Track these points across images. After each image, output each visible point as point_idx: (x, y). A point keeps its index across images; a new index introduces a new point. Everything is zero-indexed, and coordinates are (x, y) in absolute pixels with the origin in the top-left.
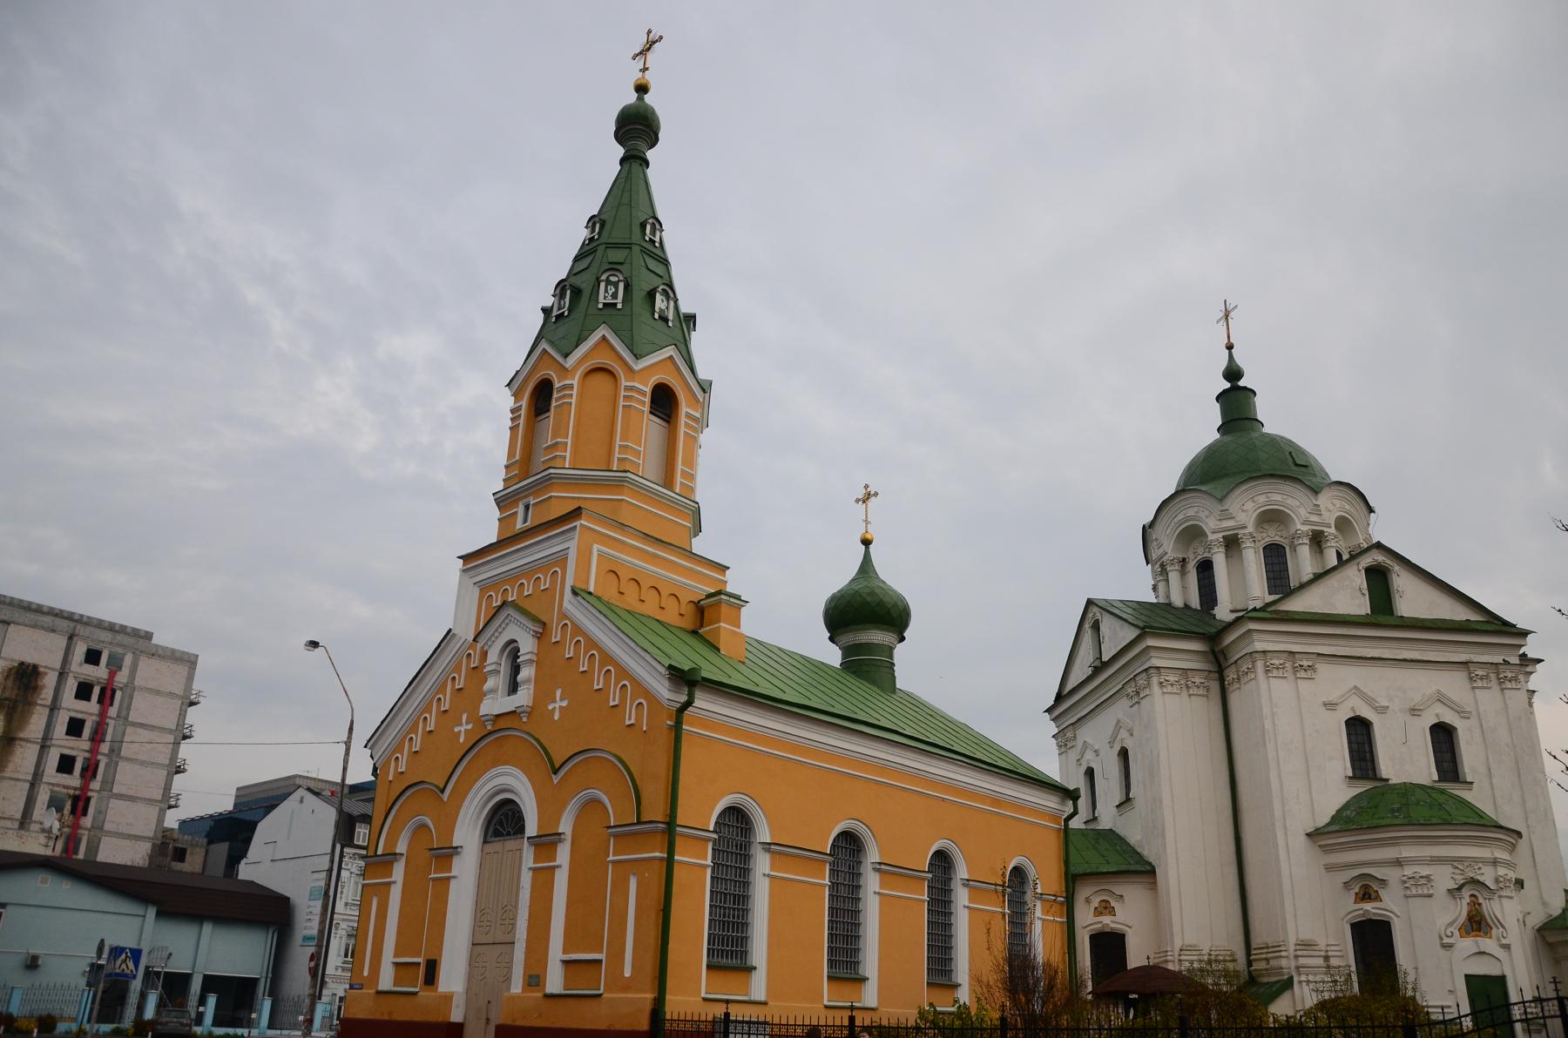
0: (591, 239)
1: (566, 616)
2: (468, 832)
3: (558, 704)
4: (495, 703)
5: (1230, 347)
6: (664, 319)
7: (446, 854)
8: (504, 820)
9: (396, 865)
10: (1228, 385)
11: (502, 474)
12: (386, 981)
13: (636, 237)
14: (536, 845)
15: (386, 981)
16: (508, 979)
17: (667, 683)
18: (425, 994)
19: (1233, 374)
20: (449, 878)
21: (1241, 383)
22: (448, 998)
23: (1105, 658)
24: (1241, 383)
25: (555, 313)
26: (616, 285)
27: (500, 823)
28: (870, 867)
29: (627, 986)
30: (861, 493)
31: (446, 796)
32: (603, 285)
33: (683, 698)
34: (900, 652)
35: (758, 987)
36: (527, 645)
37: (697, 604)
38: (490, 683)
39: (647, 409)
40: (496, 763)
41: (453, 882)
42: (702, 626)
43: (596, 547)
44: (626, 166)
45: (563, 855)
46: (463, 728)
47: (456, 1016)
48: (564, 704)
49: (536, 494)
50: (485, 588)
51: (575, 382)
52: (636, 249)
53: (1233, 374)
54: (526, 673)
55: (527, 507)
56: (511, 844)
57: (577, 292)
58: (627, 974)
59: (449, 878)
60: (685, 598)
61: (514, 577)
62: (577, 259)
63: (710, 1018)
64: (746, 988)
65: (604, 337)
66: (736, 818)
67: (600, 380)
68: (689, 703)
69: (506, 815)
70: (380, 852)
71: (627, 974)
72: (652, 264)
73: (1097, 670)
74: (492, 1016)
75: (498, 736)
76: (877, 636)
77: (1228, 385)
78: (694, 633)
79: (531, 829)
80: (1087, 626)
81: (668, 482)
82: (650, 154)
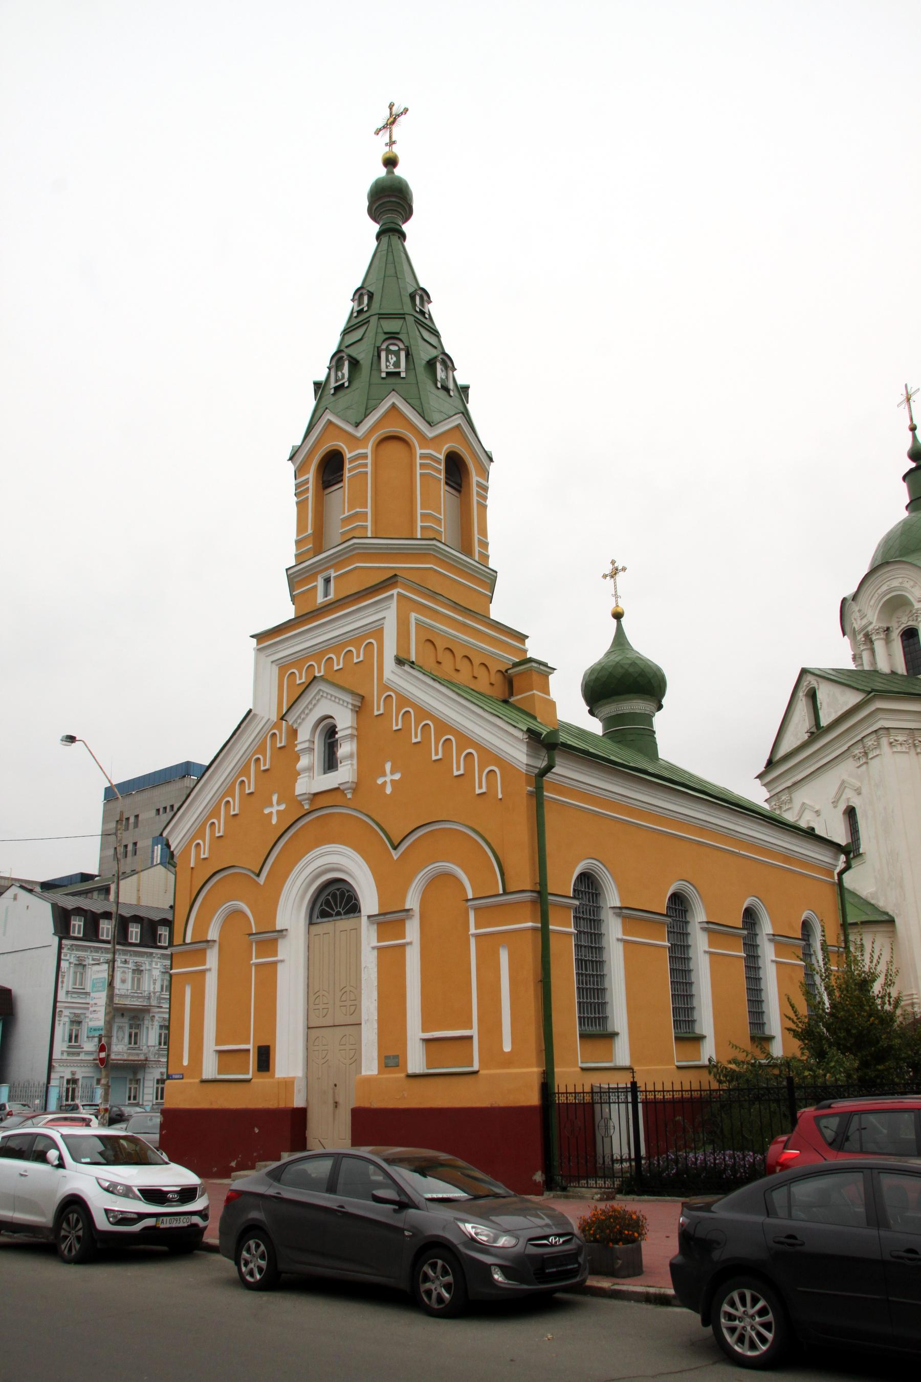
0: (360, 312)
1: (388, 688)
2: (291, 912)
3: (389, 778)
4: (311, 781)
6: (446, 389)
7: (270, 939)
8: (334, 900)
9: (209, 952)
11: (292, 550)
12: (210, 1068)
13: (408, 308)
14: (378, 924)
15: (210, 1069)
16: (356, 1060)
17: (524, 748)
18: (261, 1081)
22: (288, 1084)
23: (824, 722)
25: (333, 384)
26: (397, 354)
27: (327, 903)
28: (698, 927)
30: (608, 569)
31: (262, 880)
32: (383, 355)
33: (543, 764)
34: (660, 721)
35: (622, 1053)
36: (344, 721)
37: (504, 673)
38: (304, 762)
39: (442, 476)
40: (319, 843)
41: (280, 967)
42: (511, 694)
43: (413, 616)
45: (413, 931)
46: (275, 809)
47: (298, 1102)
48: (397, 776)
49: (336, 566)
50: (284, 667)
51: (369, 450)
52: (410, 319)
54: (345, 749)
55: (327, 581)
56: (344, 924)
57: (355, 364)
58: (507, 1048)
60: (494, 668)
61: (318, 653)
62: (346, 332)
63: (587, 1089)
64: (610, 1056)
65: (394, 406)
66: (588, 884)
67: (394, 448)
68: (549, 768)
69: (334, 896)
70: (188, 940)
71: (507, 1048)
72: (426, 335)
73: (817, 731)
74: (341, 1100)
75: (318, 817)
76: (637, 705)
78: (505, 702)
79: (369, 903)
80: (801, 694)
81: (467, 549)
82: (405, 227)
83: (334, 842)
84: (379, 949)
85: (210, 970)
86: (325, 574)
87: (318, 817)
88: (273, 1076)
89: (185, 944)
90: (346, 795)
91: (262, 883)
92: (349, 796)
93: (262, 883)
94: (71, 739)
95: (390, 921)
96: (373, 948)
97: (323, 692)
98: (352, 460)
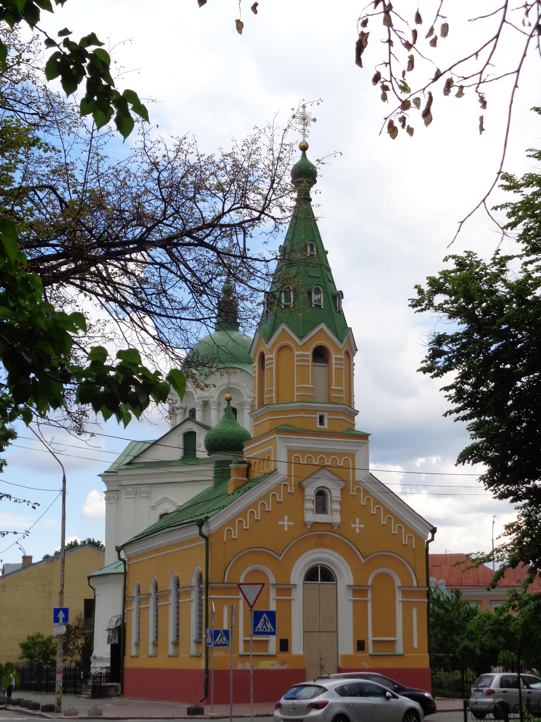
8: (320, 574)
18: (284, 655)
20: (290, 600)
22: (299, 657)
29: (416, 651)
40: (316, 546)
41: (292, 602)
55: (321, 418)
58: (416, 646)
59: (290, 600)
70: (226, 581)
71: (416, 646)
75: (320, 535)
83: (327, 548)
84: (354, 601)
85: (241, 598)
86: (322, 414)
87: (320, 535)
88: (291, 653)
89: (224, 583)
90: (334, 528)
91: (280, 559)
92: (336, 528)
93: (280, 559)
96: (350, 600)
97: (325, 475)
98: (336, 359)
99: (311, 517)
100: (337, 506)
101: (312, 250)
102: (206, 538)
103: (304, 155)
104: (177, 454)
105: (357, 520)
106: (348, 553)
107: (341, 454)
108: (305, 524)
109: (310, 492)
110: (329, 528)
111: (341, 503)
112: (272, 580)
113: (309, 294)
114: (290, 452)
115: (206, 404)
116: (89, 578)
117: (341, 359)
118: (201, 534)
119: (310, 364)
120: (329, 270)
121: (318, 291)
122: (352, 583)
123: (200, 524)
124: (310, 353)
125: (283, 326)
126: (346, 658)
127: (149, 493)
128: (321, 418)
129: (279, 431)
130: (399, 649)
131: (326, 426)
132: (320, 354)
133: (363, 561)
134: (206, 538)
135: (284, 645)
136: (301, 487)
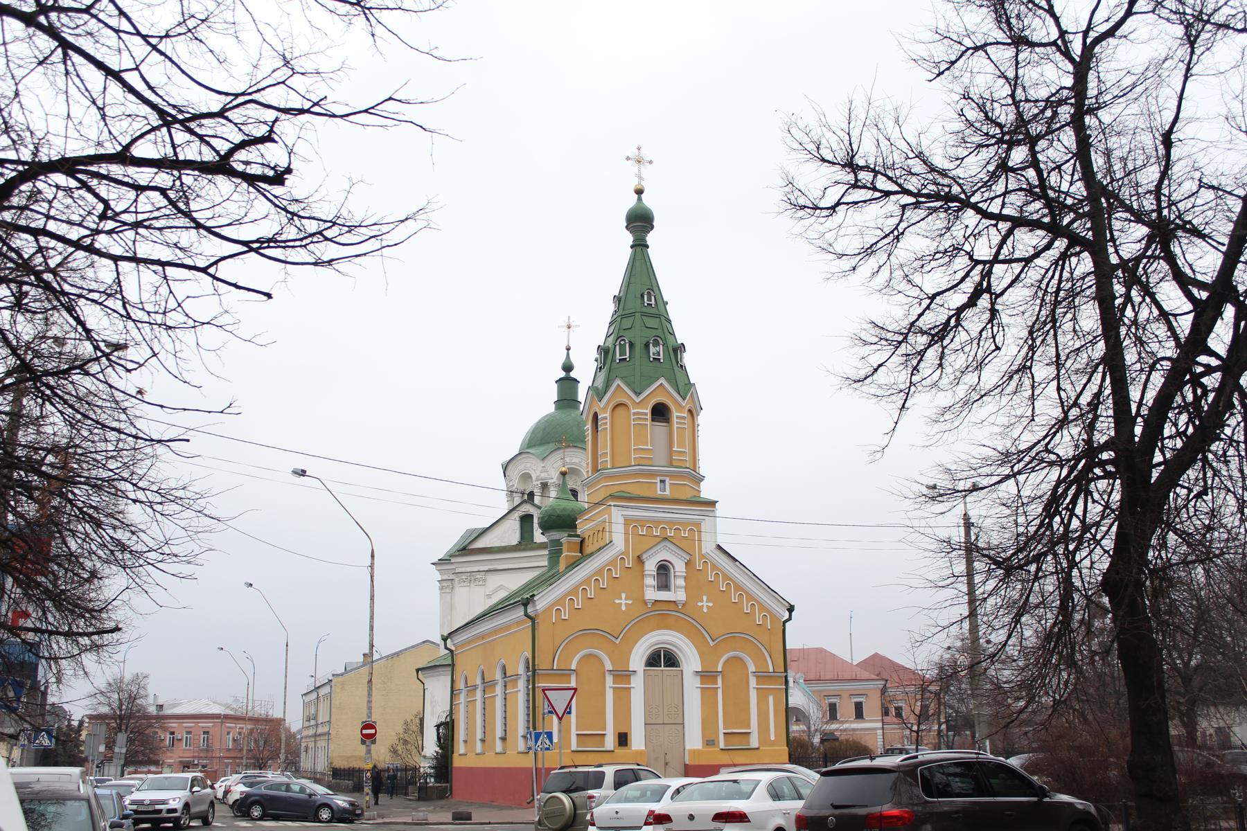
5: (568, 349)
7: (623, 675)
8: (663, 659)
10: (563, 374)
18: (622, 751)
19: (568, 367)
21: (573, 374)
24: (573, 374)
29: (773, 744)
36: (679, 567)
44: (639, 249)
53: (568, 367)
77: (563, 374)
87: (663, 614)
94: (303, 473)
95: (707, 676)
99: (652, 594)
100: (681, 582)
101: (649, 299)
102: (532, 619)
103: (640, 199)
104: (514, 539)
105: (705, 598)
106: (694, 634)
107: (685, 524)
108: (645, 603)
109: (651, 566)
110: (672, 607)
111: (685, 578)
112: (609, 666)
113: (647, 346)
114: (628, 521)
115: (545, 486)
116: (418, 671)
117: (684, 418)
118: (526, 615)
119: (649, 422)
120: (669, 321)
121: (656, 344)
122: (699, 669)
123: (526, 603)
124: (648, 411)
125: (618, 382)
126: (694, 753)
127: (485, 581)
128: (663, 482)
129: (612, 497)
130: (754, 742)
131: (667, 492)
132: (660, 412)
133: (712, 644)
134: (532, 619)
135: (623, 739)
136: (640, 560)
